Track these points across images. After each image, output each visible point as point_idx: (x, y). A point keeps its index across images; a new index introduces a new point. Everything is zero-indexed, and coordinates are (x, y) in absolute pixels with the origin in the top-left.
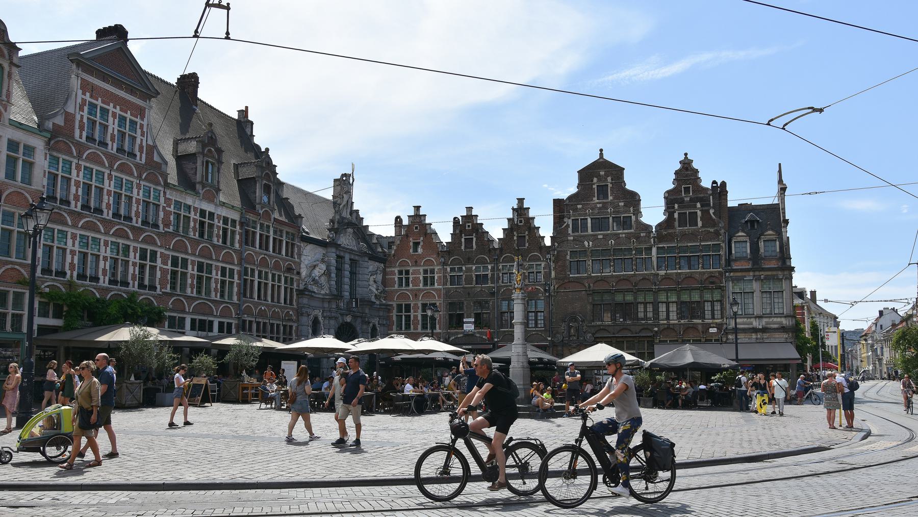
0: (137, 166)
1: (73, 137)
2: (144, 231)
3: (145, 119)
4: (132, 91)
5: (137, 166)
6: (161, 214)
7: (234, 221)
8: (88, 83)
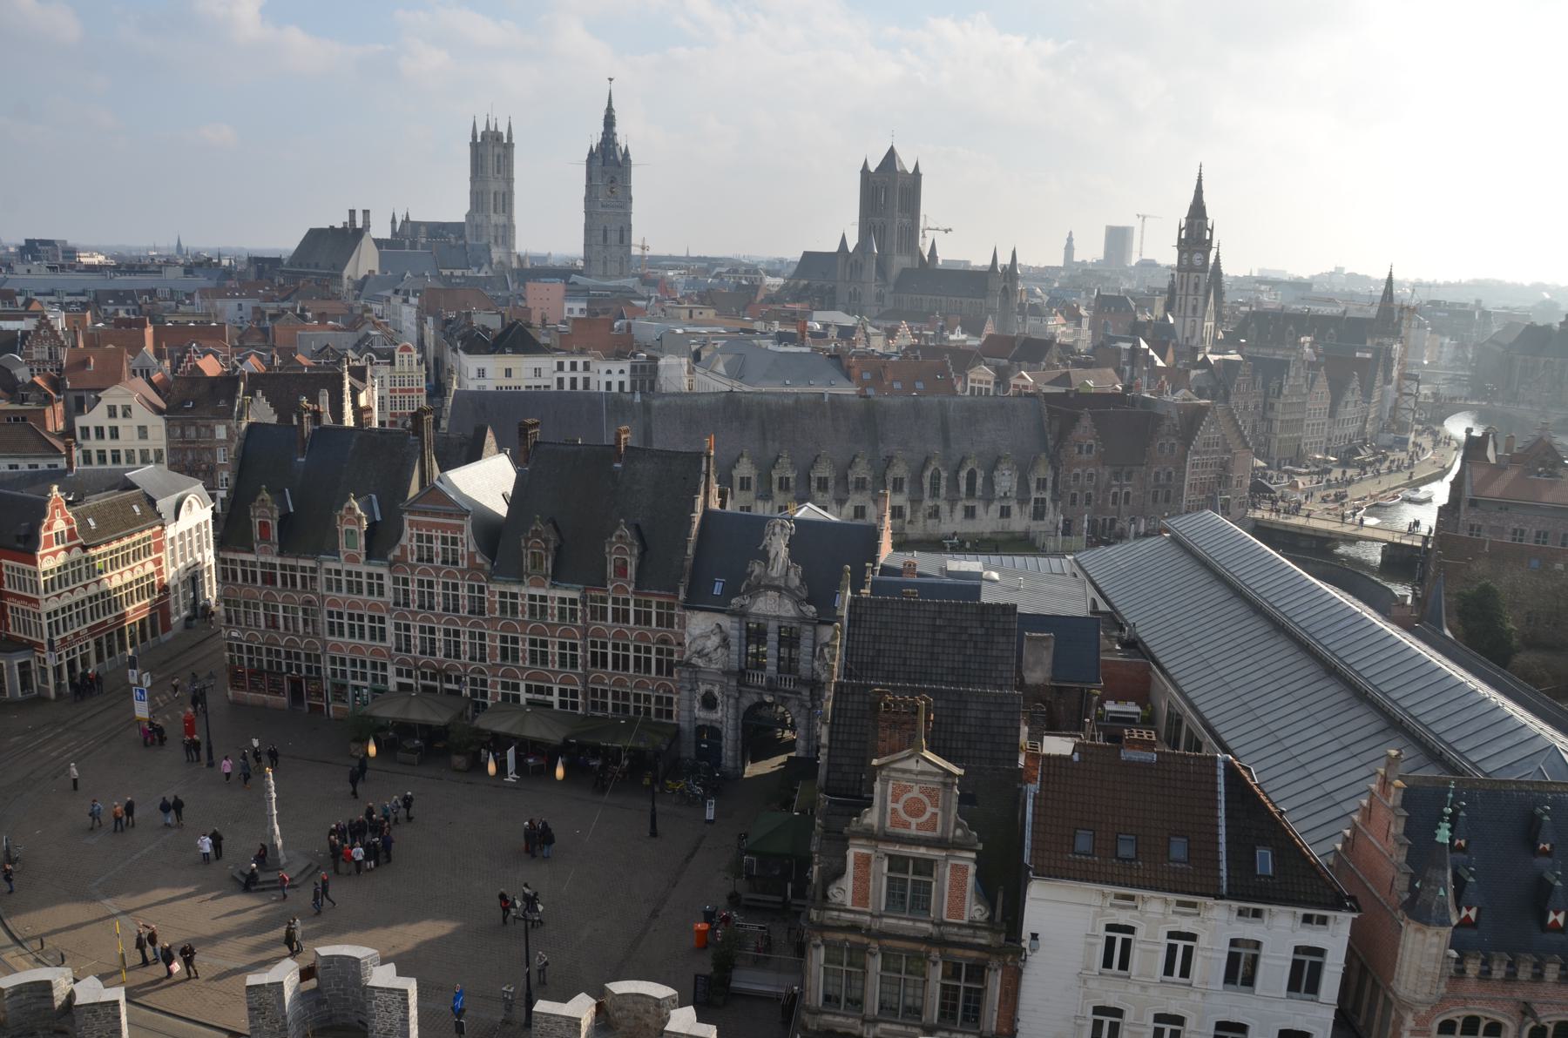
0: (461, 571)
1: (407, 561)
2: (471, 618)
3: (465, 533)
4: (449, 515)
5: (461, 571)
6: (486, 604)
7: (573, 602)
8: (414, 521)
